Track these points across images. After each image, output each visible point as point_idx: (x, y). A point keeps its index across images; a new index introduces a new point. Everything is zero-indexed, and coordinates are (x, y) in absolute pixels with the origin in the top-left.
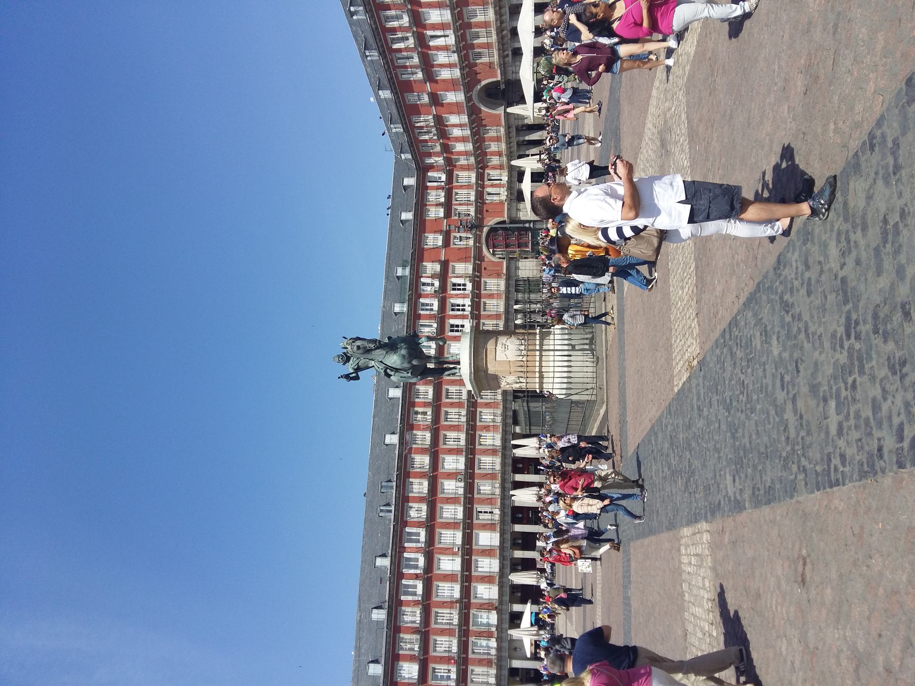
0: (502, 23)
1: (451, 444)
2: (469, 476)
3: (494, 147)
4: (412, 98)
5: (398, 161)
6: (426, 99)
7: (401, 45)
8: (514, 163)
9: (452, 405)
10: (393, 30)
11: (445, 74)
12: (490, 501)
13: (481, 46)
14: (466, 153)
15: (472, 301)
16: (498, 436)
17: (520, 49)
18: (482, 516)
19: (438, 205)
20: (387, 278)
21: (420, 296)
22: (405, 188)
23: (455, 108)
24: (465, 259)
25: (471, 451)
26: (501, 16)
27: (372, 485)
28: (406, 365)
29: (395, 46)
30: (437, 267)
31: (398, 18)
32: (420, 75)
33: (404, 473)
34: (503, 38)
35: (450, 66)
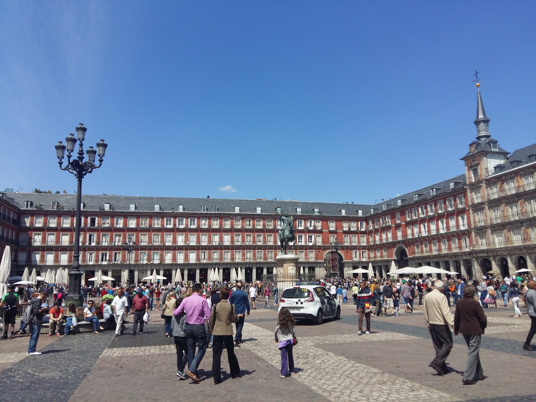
0: (432, 258)
1: (236, 238)
2: (221, 248)
3: (378, 254)
4: (398, 215)
5: (369, 207)
6: (398, 222)
7: (420, 211)
8: (370, 264)
9: (254, 238)
10: (426, 208)
11: (409, 231)
12: (210, 258)
13: (422, 248)
14: (375, 241)
15: (304, 246)
16: (240, 261)
17: (422, 266)
18: (203, 254)
19: (349, 228)
20: (313, 203)
21: (305, 220)
22: (357, 211)
23: (395, 236)
24: (323, 242)
25: (232, 248)
26: (435, 257)
27: (215, 201)
28: (285, 237)
29: (420, 208)
30: (319, 228)
31: (432, 210)
32: (408, 219)
33: (222, 217)
34: (426, 258)
35: (413, 234)
